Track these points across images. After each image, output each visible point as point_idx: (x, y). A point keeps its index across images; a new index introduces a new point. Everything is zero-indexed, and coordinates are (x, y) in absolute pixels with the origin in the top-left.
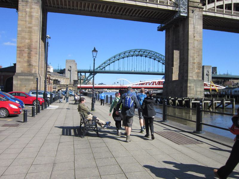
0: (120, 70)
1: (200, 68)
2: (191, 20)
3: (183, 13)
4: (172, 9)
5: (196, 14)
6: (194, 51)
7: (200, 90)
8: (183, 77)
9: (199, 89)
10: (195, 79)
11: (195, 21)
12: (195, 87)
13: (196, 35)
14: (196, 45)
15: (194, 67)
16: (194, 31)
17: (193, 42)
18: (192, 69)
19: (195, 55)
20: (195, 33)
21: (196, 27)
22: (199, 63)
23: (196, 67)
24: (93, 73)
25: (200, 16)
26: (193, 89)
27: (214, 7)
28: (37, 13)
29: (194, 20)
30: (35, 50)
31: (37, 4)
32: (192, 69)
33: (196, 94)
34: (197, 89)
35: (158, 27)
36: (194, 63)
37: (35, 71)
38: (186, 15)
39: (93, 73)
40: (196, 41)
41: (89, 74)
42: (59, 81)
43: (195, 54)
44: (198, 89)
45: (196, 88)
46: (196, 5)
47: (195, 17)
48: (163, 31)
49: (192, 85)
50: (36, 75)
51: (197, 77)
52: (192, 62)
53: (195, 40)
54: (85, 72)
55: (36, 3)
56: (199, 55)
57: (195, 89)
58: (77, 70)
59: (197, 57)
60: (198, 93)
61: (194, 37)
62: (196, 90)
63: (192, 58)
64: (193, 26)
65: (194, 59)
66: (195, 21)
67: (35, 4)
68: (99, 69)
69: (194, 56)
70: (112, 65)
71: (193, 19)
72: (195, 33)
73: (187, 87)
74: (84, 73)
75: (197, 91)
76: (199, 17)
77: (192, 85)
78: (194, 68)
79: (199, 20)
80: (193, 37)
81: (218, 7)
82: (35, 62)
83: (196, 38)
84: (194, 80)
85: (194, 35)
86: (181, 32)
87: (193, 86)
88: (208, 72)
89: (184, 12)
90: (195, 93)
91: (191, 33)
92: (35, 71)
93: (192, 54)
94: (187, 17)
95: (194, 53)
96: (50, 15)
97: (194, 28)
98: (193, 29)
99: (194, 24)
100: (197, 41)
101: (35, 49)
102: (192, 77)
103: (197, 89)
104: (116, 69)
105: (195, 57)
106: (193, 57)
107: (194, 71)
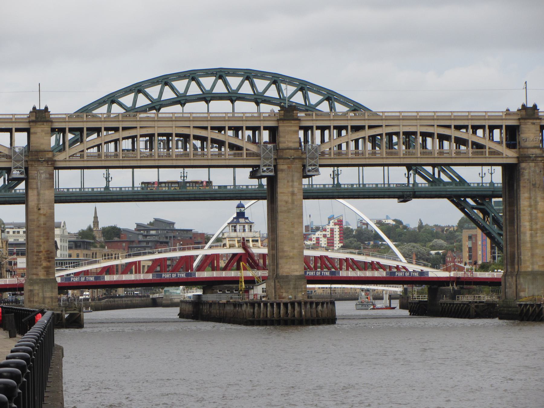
1: (50, 259)
5: (42, 171)
6: (39, 232)
7: (51, 295)
9: (48, 294)
10: (42, 277)
11: (39, 184)
13: (41, 206)
14: (42, 223)
15: (41, 258)
16: (39, 200)
17: (38, 218)
19: (41, 239)
21: (42, 192)
22: (48, 251)
23: (43, 258)
26: (38, 294)
29: (37, 183)
32: (37, 262)
33: (44, 303)
36: (40, 252)
43: (42, 238)
44: (47, 293)
45: (43, 292)
47: (40, 176)
51: (47, 274)
52: (36, 250)
56: (48, 239)
57: (41, 294)
60: (47, 300)
61: (39, 209)
62: (44, 295)
63: (35, 244)
65: (40, 246)
69: (40, 241)
72: (41, 202)
75: (44, 298)
78: (39, 260)
79: (48, 180)
80: (36, 210)
83: (42, 212)
84: (41, 280)
87: (38, 290)
95: (39, 236)
98: (36, 197)
99: (37, 188)
100: (44, 215)
102: (37, 275)
103: (45, 294)
106: (37, 242)
107: (41, 265)
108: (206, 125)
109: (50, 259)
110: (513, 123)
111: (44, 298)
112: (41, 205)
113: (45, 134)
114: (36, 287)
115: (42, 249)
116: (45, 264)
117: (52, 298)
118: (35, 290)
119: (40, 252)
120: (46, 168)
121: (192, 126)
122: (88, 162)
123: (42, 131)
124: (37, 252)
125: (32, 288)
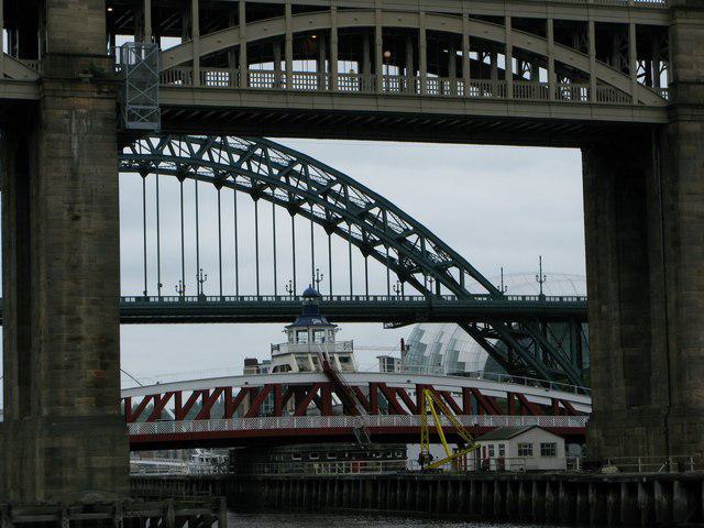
11: (75, 146)
23: (86, 356)
25: (106, 119)
26: (73, 461)
27: (190, 63)
34: (93, 459)
40: (85, 238)
57: (81, 460)
61: (76, 218)
63: (64, 317)
66: (75, 146)
71: (63, 136)
75: (91, 471)
85: (71, 209)
102: (70, 405)
105: (82, 309)
109: (108, 360)
110: (656, 20)
111: (91, 471)
113: (90, 8)
114: (69, 442)
119: (78, 339)
120: (96, 101)
121: (466, 12)
122: (251, 96)
125: (56, 444)
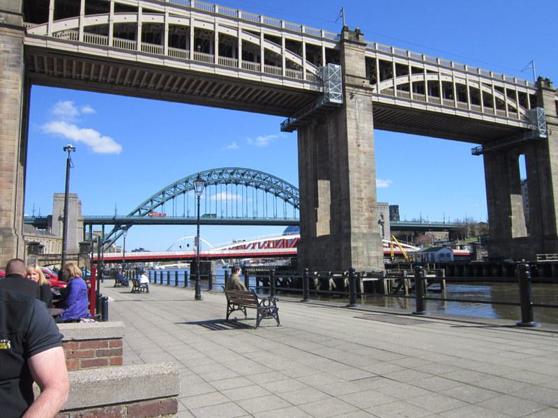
0: (188, 217)
2: (351, 112)
3: (333, 98)
4: (309, 89)
6: (360, 173)
7: (376, 255)
8: (340, 228)
9: (373, 253)
10: (365, 231)
11: (357, 115)
12: (365, 249)
14: (362, 163)
15: (362, 207)
18: (358, 211)
20: (361, 138)
21: (361, 125)
22: (370, 198)
23: (365, 206)
24: (122, 224)
25: (368, 105)
26: (363, 253)
27: (393, 88)
28: (13, 88)
29: (355, 113)
30: (9, 172)
31: (14, 68)
33: (369, 265)
35: (283, 124)
36: (361, 199)
37: (8, 223)
38: (340, 102)
39: (122, 224)
41: (114, 226)
42: (42, 247)
44: (373, 252)
46: (358, 82)
47: (359, 106)
48: (292, 132)
49: (360, 244)
50: (9, 232)
51: (369, 227)
53: (360, 151)
54: (103, 222)
55: (13, 66)
56: (369, 183)
57: (365, 253)
58: (83, 218)
59: (365, 187)
60: (372, 261)
61: (359, 146)
62: (368, 253)
64: (354, 123)
65: (361, 191)
66: (357, 115)
67: (11, 68)
68: (137, 213)
70: (169, 204)
71: (353, 110)
73: (349, 248)
74: (101, 226)
75: (369, 258)
76: (366, 106)
77: (360, 244)
79: (367, 112)
80: (355, 145)
81: (399, 87)
82: (8, 200)
84: (364, 234)
85: (357, 142)
86: (331, 136)
87: (363, 248)
88: (382, 216)
89: (336, 95)
90: (366, 261)
91: (351, 137)
92: (8, 223)
93: (356, 180)
94: (343, 106)
95: (359, 179)
96: (35, 89)
97: (357, 128)
101: (7, 170)
104: (179, 215)
105: (363, 186)
106: (358, 186)
107: (362, 216)
108: (490, 83)
112: (361, 141)
115: (363, 195)
116: (367, 214)
117: (377, 257)
118: (359, 247)
123: (356, 54)
124: (359, 199)
